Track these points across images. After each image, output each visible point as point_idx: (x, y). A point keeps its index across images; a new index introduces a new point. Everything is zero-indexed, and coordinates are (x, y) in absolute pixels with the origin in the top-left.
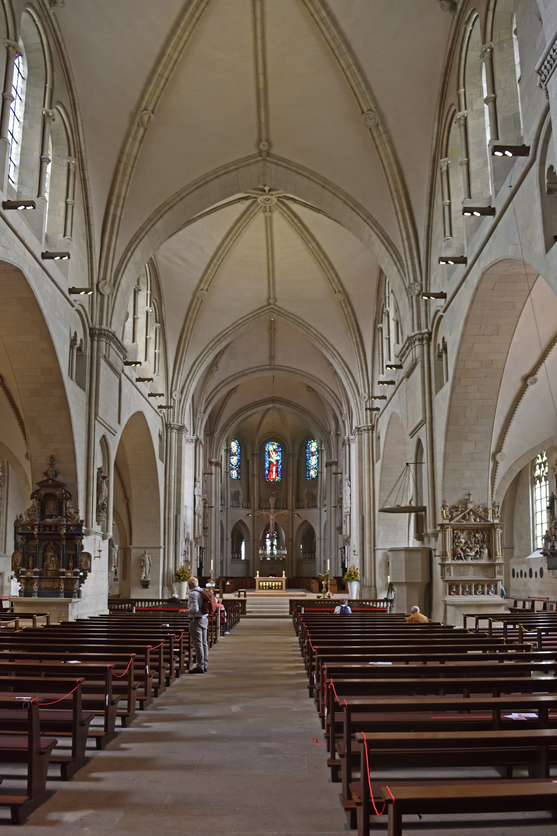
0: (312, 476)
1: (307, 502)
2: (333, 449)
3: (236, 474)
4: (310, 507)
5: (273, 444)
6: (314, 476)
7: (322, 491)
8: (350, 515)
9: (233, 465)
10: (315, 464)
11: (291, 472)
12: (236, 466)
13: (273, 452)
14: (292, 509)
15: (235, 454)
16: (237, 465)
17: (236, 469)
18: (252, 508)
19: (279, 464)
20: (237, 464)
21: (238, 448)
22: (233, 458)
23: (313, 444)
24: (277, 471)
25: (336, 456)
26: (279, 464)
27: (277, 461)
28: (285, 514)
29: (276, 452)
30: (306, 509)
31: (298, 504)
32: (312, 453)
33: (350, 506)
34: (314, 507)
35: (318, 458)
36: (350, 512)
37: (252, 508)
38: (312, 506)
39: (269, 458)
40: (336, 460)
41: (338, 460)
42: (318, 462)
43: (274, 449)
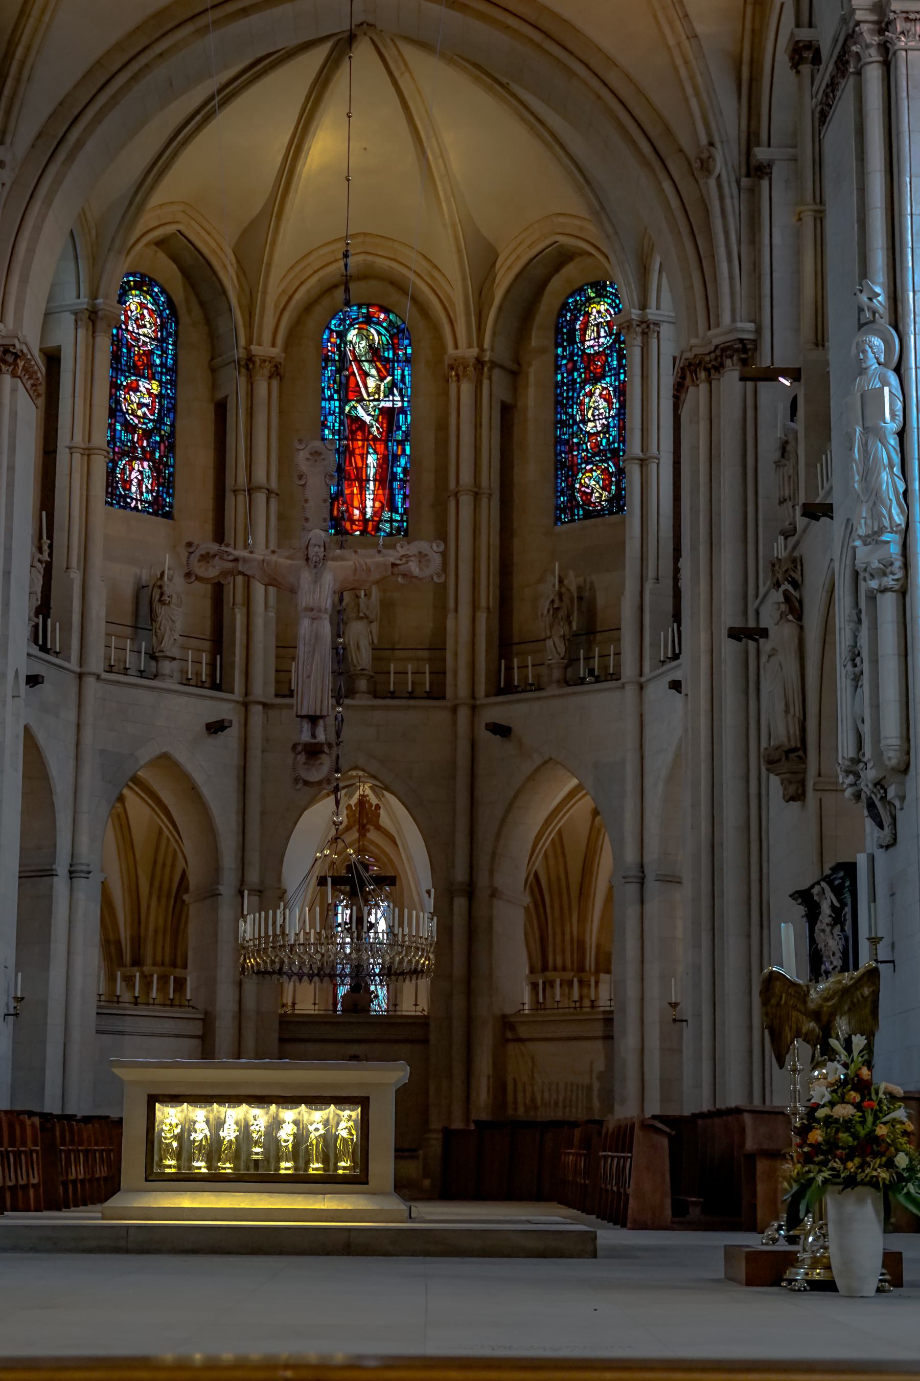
0: (588, 502)
1: (562, 648)
2: (724, 267)
3: (147, 483)
4: (582, 681)
5: (369, 320)
6: (599, 495)
7: (651, 573)
8: (903, 593)
9: (130, 428)
10: (606, 428)
11: (466, 477)
12: (147, 434)
13: (366, 366)
14: (473, 697)
15: (151, 365)
16: (157, 429)
17: (147, 456)
18: (238, 686)
19: (399, 436)
20: (159, 421)
21: (163, 327)
22: (136, 390)
23: (594, 309)
24: (385, 477)
25: (743, 308)
26: (399, 436)
27: (389, 415)
28: (414, 567)
29: (386, 367)
30: (552, 690)
31: (509, 669)
32: (590, 359)
33: (899, 519)
34: (598, 680)
35: (621, 391)
36: (906, 566)
37: (238, 686)
38: (591, 672)
39: (344, 401)
40: (746, 328)
41: (758, 331)
42: (621, 413)
43: (370, 346)
